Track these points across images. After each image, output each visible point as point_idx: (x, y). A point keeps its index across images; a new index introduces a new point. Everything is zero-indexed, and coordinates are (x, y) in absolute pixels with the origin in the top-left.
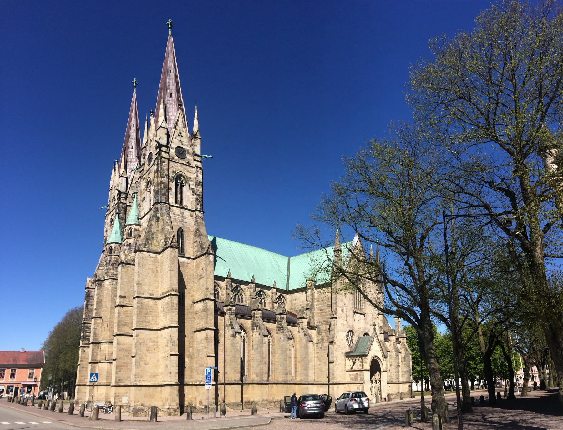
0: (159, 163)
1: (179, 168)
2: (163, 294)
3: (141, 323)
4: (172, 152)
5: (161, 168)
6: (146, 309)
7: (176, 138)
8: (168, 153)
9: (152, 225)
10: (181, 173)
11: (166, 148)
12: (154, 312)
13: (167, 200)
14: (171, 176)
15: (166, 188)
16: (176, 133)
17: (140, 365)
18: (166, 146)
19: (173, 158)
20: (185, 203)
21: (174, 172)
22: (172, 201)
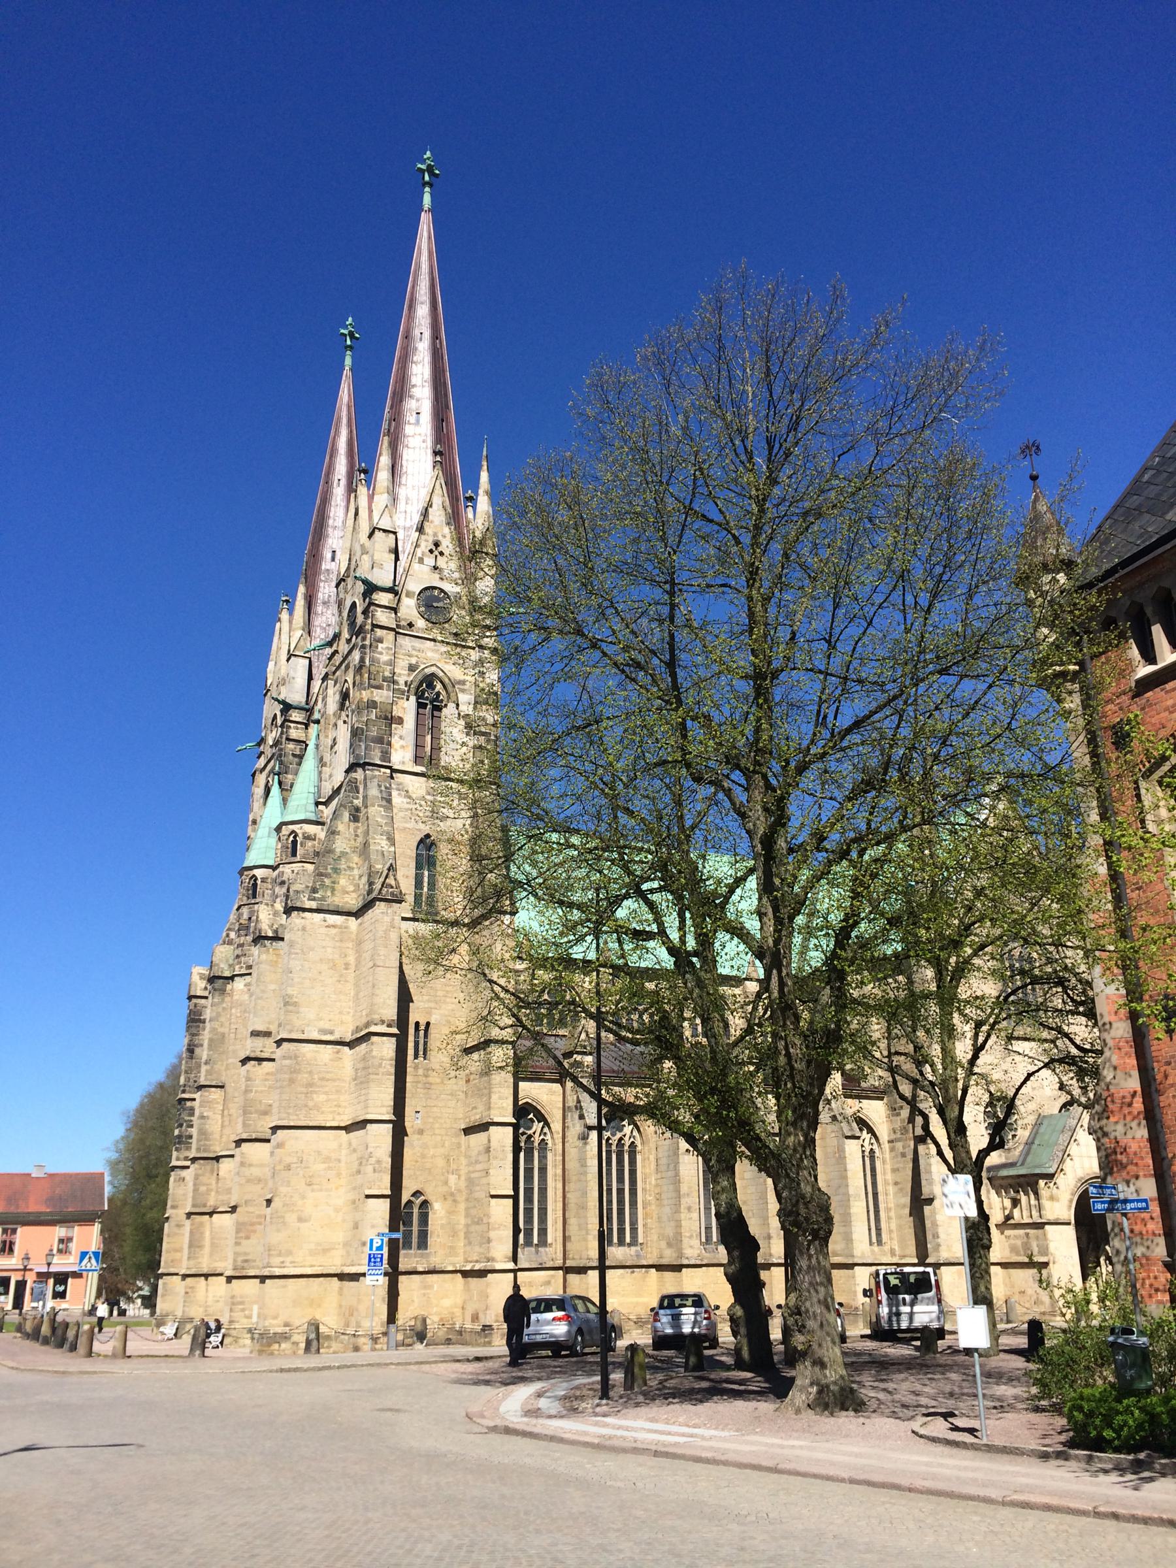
0: (367, 642)
1: (430, 654)
2: (358, 1029)
3: (291, 1111)
4: (408, 607)
5: (372, 660)
6: (310, 1072)
7: (421, 561)
8: (395, 610)
9: (338, 833)
10: (433, 669)
11: (391, 596)
12: (334, 1080)
13: (386, 756)
14: (401, 680)
15: (386, 718)
16: (423, 544)
17: (284, 1223)
18: (391, 590)
19: (411, 625)
20: (445, 760)
21: (412, 668)
22: (402, 754)
